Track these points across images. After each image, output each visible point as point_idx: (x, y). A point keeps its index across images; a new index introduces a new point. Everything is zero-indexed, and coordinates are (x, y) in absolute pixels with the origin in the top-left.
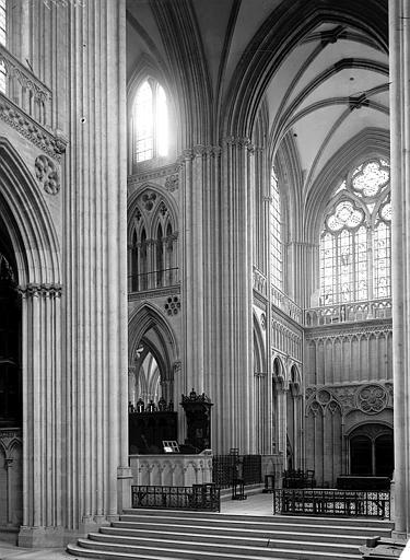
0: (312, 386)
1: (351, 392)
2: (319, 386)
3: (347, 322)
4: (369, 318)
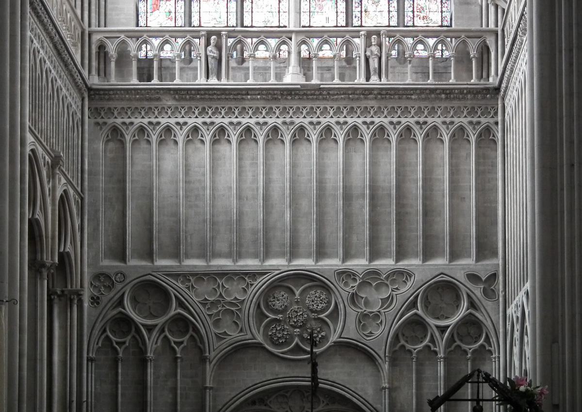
0: (108, 264)
1: (234, 291)
3: (225, 82)
4: (292, 77)
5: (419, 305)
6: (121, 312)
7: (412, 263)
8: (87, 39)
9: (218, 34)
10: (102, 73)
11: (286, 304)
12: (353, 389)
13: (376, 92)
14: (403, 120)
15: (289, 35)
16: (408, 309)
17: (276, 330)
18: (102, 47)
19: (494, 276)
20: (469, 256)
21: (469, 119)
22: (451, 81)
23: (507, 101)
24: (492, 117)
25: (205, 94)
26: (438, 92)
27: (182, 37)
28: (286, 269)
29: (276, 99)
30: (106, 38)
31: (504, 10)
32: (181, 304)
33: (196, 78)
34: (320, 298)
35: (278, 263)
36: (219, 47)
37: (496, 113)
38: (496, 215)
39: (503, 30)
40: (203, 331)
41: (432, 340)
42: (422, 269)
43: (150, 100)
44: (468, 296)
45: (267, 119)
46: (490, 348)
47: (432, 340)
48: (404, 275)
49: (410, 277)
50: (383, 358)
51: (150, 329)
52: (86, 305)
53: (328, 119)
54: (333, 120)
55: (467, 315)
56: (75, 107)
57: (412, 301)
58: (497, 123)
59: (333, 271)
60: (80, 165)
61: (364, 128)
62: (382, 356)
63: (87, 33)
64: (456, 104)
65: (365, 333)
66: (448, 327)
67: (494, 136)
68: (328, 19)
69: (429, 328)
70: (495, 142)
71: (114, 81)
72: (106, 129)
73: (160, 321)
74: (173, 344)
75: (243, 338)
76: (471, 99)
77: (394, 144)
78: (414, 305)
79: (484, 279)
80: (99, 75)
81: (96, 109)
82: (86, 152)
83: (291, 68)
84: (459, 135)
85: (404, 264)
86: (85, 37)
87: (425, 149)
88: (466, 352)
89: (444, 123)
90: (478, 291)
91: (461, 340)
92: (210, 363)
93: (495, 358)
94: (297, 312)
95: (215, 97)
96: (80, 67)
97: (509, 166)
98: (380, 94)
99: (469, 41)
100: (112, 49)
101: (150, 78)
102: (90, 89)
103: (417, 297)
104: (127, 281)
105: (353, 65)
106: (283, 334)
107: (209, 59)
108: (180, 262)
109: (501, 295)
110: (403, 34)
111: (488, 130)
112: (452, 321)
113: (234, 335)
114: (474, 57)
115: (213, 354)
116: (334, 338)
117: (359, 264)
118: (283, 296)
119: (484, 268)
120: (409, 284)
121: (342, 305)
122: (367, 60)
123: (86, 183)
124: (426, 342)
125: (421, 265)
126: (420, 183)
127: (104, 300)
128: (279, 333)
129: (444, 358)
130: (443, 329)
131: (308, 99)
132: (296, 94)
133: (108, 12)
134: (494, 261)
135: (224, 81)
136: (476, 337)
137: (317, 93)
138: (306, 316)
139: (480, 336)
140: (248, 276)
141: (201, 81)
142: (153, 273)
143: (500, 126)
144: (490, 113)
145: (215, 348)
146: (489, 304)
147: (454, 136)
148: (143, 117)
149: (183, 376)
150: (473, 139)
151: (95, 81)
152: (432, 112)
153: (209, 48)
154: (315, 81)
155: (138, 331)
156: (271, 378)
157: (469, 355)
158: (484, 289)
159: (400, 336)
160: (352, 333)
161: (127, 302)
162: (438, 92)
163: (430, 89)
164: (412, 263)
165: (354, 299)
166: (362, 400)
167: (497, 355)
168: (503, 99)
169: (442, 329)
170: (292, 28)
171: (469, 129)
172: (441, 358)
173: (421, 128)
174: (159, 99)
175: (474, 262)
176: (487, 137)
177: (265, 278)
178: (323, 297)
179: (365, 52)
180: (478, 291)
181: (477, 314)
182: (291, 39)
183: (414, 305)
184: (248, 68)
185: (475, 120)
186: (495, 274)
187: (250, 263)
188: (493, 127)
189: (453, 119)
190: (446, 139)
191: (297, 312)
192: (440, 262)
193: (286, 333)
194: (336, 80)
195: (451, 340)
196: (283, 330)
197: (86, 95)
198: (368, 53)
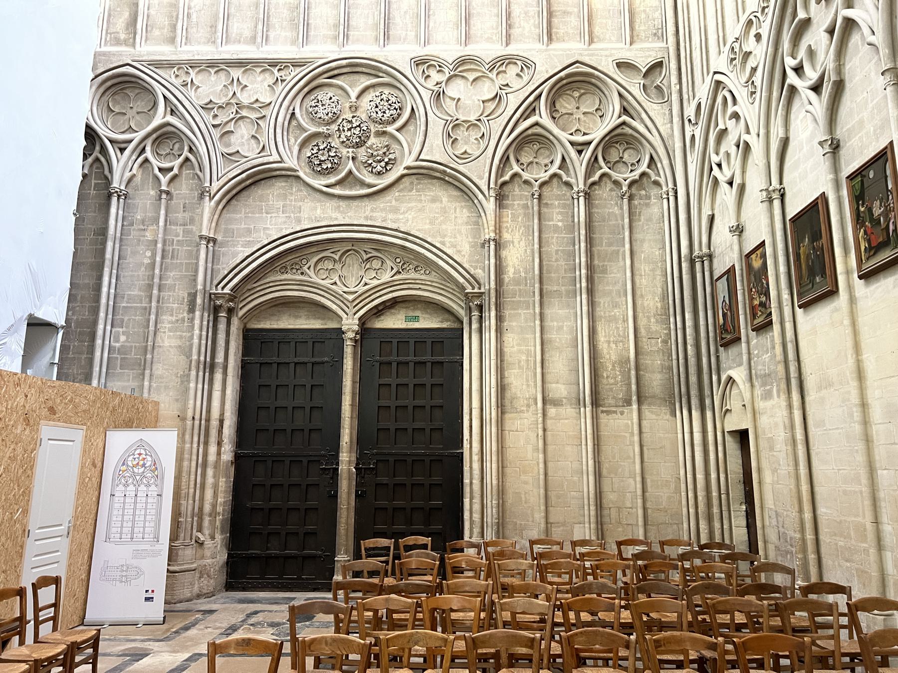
11: (335, 110)
12: (438, 245)
16: (525, 116)
17: (319, 150)
34: (387, 101)
35: (324, 50)
40: (202, 149)
46: (657, 178)
50: (486, 193)
62: (485, 188)
65: (456, 153)
75: (265, 160)
92: (211, 199)
94: (350, 122)
106: (329, 156)
108: (176, 47)
113: (250, 154)
115: (216, 185)
116: (409, 161)
118: (331, 98)
125: (546, 50)
128: (323, 154)
130: (580, 148)
136: (632, 165)
138: (365, 128)
140: (278, 68)
145: (220, 175)
156: (309, 227)
160: (436, 151)
166: (451, 262)
169: (579, 148)
181: (635, 124)
191: (350, 122)
193: (332, 154)
195: (593, 163)
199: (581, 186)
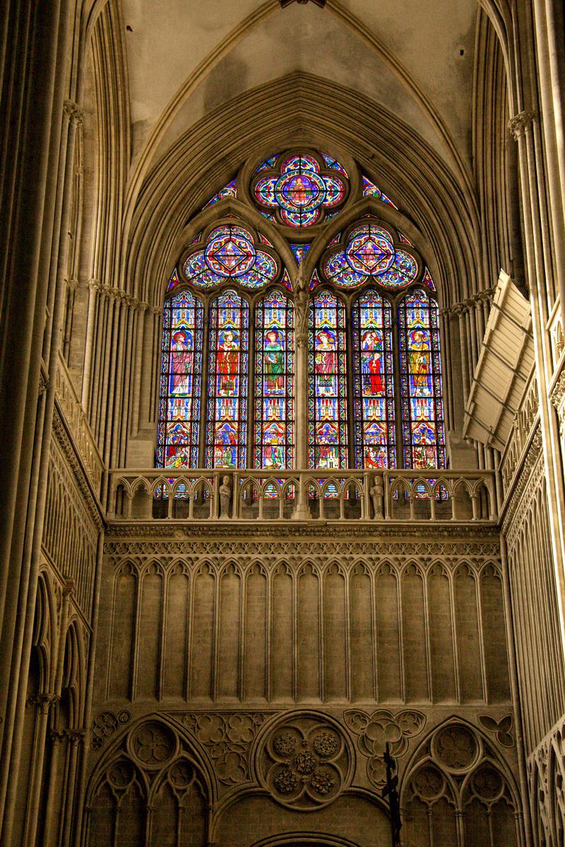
1: (240, 730)
2: (142, 706)
3: (236, 519)
5: (432, 750)
6: (122, 756)
7: (422, 704)
8: (107, 479)
9: (231, 475)
10: (119, 511)
13: (380, 529)
14: (408, 557)
15: (297, 476)
16: (420, 755)
18: (121, 487)
19: (508, 721)
20: (481, 697)
21: (472, 556)
22: (452, 519)
23: (509, 538)
24: (495, 554)
25: (217, 530)
26: (440, 529)
27: (195, 478)
28: (293, 709)
29: (284, 535)
30: (126, 478)
31: (499, 453)
32: (186, 748)
33: (207, 516)
35: (284, 702)
36: (231, 486)
37: (498, 551)
38: (505, 653)
39: (500, 472)
40: (207, 777)
41: (449, 792)
42: (436, 711)
43: (165, 535)
44: (484, 742)
45: (276, 555)
47: (449, 792)
48: (418, 716)
49: (422, 718)
51: (152, 775)
52: (87, 747)
53: (333, 556)
54: (339, 557)
55: (482, 764)
56: (92, 540)
57: (424, 745)
58: (500, 561)
59: (341, 712)
60: (92, 600)
61: (369, 564)
63: (107, 473)
64: (458, 541)
66: (464, 776)
67: (497, 573)
68: (331, 463)
69: (444, 778)
70: (499, 579)
71: (130, 518)
72: (121, 565)
73: (163, 767)
74: (175, 793)
75: (248, 785)
76: (473, 537)
77: (399, 580)
78: (427, 749)
79: (498, 723)
80: (116, 513)
81: (112, 544)
82: (99, 586)
83: (298, 506)
84: (464, 571)
85: (414, 705)
86: (105, 478)
87: (430, 585)
88: (485, 806)
89: (448, 559)
90: (493, 736)
91: (479, 793)
93: (517, 815)
94: (304, 756)
95: (226, 533)
96: (98, 502)
97: (515, 602)
98: (384, 531)
99: (466, 481)
100: (131, 489)
101: (164, 516)
102: (105, 524)
103: (430, 740)
104: (131, 721)
105: (357, 505)
107: (222, 497)
109: (518, 740)
110: (405, 475)
111: (491, 567)
112: (469, 769)
113: (240, 782)
114: (474, 497)
116: (345, 787)
117: (367, 704)
119: (498, 711)
120: (421, 727)
121: (352, 748)
122: (371, 499)
123: (97, 618)
124: (442, 793)
126: (427, 620)
127: (107, 742)
129: (464, 813)
130: (459, 779)
131: (315, 535)
132: (304, 531)
133: (128, 455)
134: (507, 703)
135: (235, 518)
137: (324, 529)
139: (498, 790)
141: (213, 518)
142: (159, 713)
143: (503, 563)
144: (492, 550)
146: (506, 752)
147: (459, 572)
148: (156, 553)
149: (184, 830)
150: (477, 576)
151: (111, 517)
152: (436, 548)
153: (222, 487)
154: (321, 519)
155: (140, 777)
157: (489, 811)
158: (500, 734)
159: (414, 786)
161: (130, 745)
162: (440, 529)
163: (433, 527)
164: (422, 704)
165: (364, 739)
167: (519, 810)
168: (505, 537)
170: (300, 468)
171: (473, 566)
172: (459, 813)
173: (426, 565)
174: (172, 535)
175: (486, 705)
176: (490, 573)
177: (274, 717)
178: (332, 739)
179: (369, 491)
180: (493, 736)
181: (494, 763)
182: (298, 479)
183: (427, 749)
184: (258, 509)
185: (478, 557)
186: (509, 717)
187: (259, 703)
188: (496, 564)
189: (456, 556)
190: (451, 575)
191: (304, 756)
192: (450, 703)
194: (342, 518)
195: (469, 791)
196: (291, 777)
197: (102, 531)
198: (372, 493)
199: (460, 809)
